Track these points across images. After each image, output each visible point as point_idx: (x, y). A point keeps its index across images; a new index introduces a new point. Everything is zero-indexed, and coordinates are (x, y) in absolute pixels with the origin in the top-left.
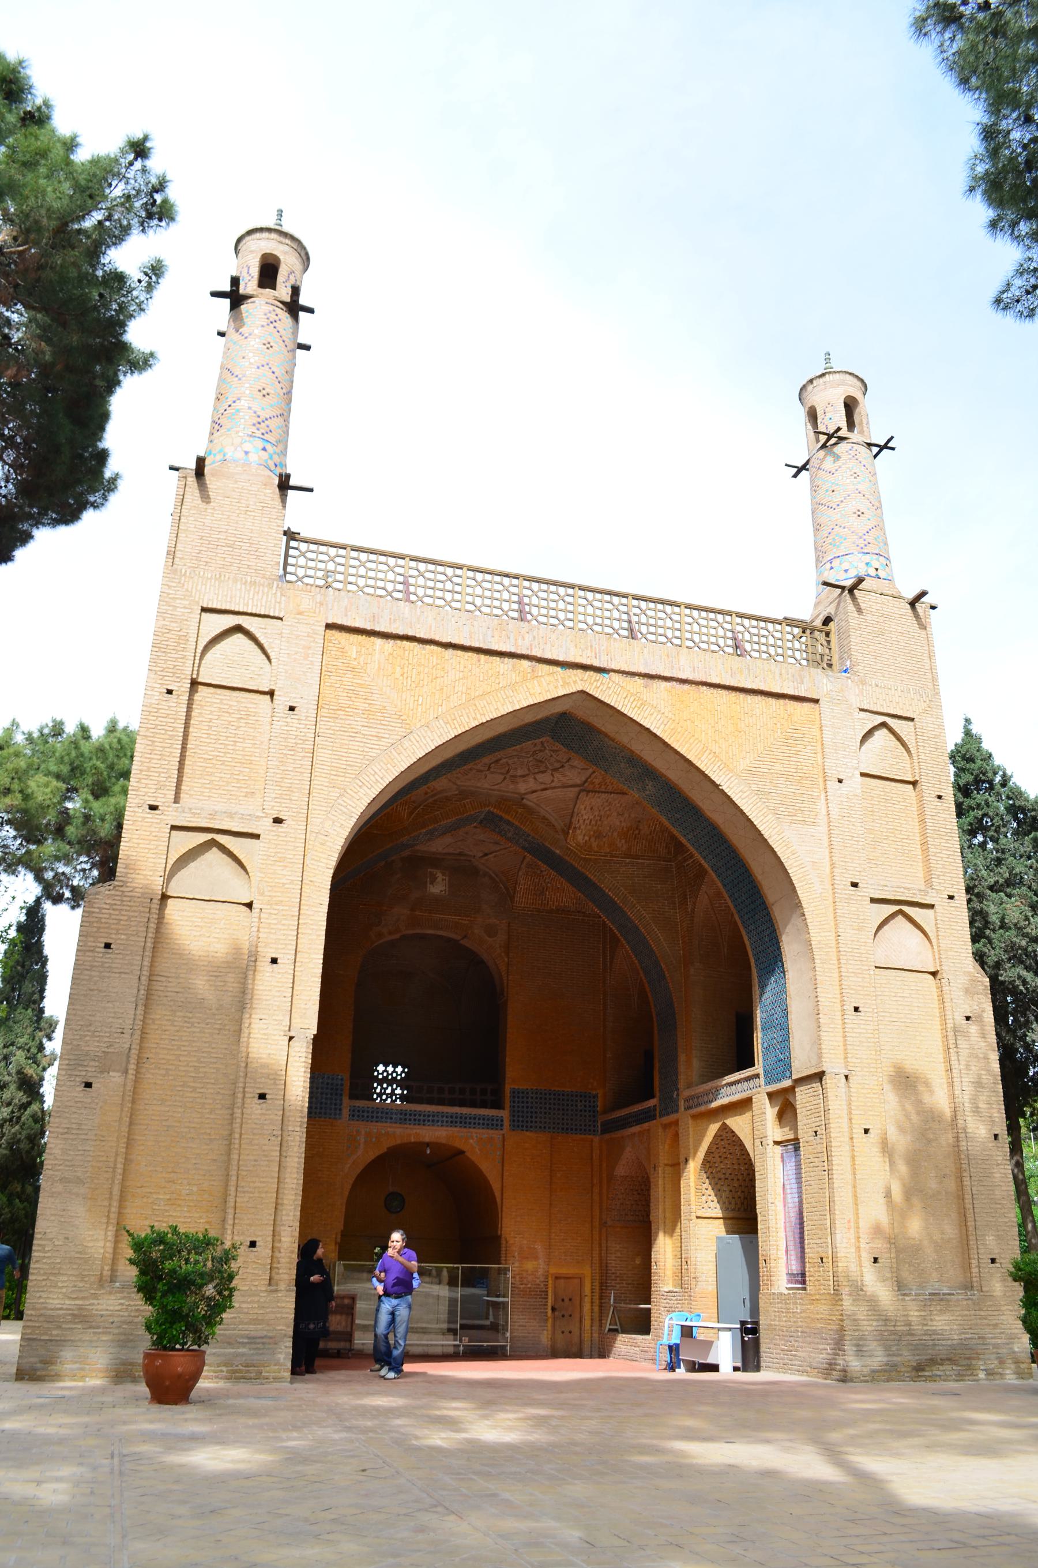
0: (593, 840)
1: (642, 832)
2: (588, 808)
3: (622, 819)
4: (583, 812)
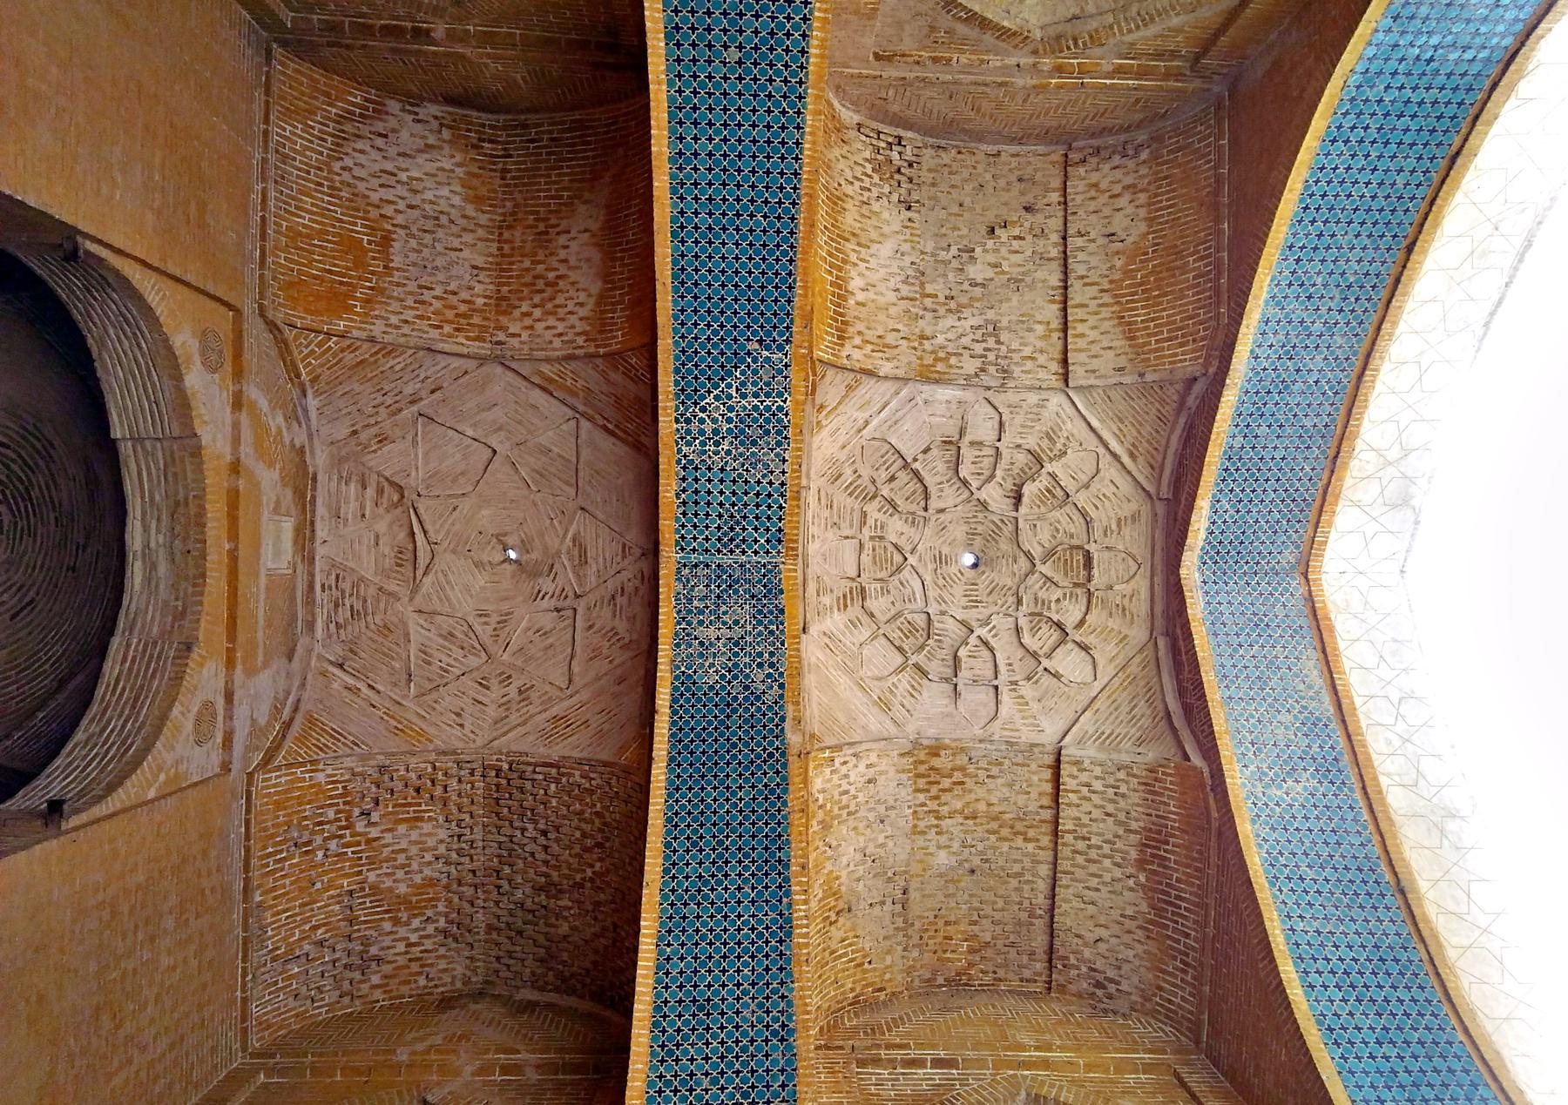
0: (820, 815)
1: (833, 928)
2: (871, 773)
3: (852, 867)
4: (862, 767)
